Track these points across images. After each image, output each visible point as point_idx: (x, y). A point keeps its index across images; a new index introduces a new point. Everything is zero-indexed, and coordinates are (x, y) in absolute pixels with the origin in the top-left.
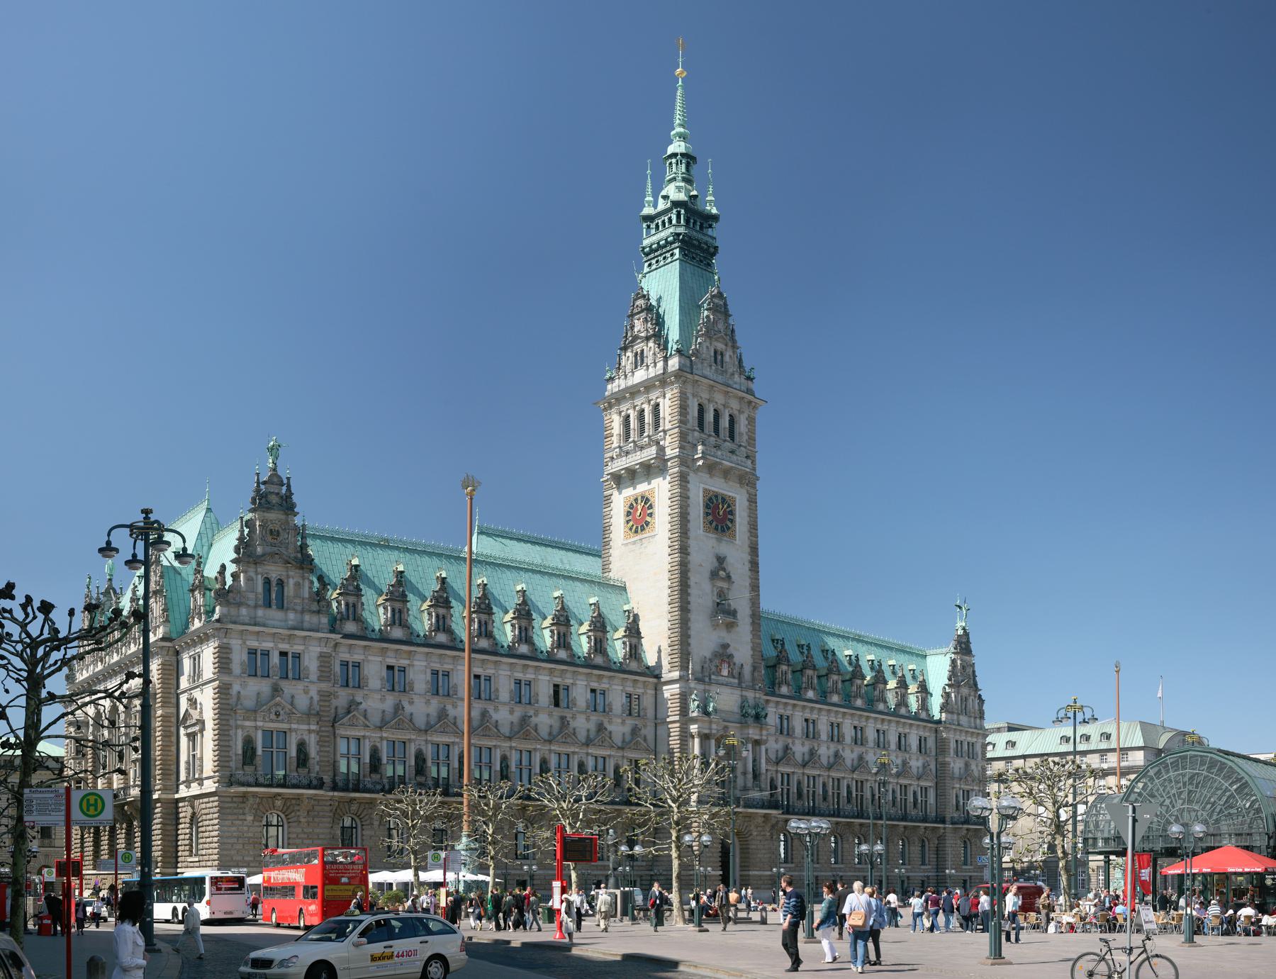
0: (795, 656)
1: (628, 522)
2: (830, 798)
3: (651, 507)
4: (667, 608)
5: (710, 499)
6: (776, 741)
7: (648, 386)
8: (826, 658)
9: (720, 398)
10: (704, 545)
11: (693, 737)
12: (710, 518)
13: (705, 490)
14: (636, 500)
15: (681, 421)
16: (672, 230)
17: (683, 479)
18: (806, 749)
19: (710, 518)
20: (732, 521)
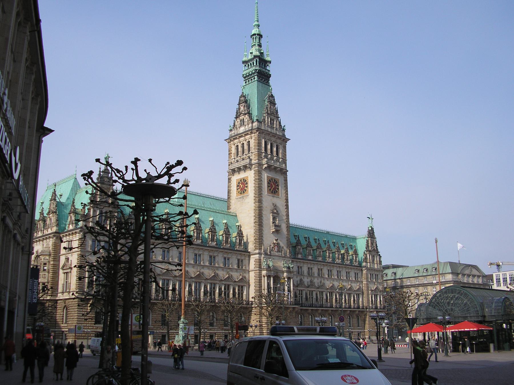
0: (304, 243)
1: (238, 189)
2: (319, 300)
3: (247, 183)
4: (253, 224)
5: (270, 180)
6: (297, 277)
7: (246, 133)
8: (316, 242)
9: (273, 139)
10: (268, 200)
11: (264, 277)
12: (270, 188)
13: (268, 177)
14: (241, 180)
15: (258, 149)
16: (254, 68)
17: (259, 173)
18: (309, 280)
19: (270, 188)
20: (278, 189)
